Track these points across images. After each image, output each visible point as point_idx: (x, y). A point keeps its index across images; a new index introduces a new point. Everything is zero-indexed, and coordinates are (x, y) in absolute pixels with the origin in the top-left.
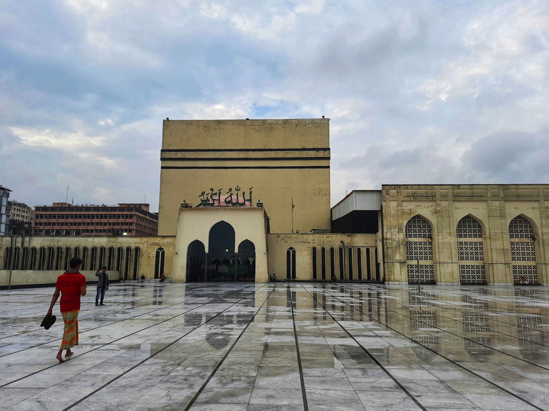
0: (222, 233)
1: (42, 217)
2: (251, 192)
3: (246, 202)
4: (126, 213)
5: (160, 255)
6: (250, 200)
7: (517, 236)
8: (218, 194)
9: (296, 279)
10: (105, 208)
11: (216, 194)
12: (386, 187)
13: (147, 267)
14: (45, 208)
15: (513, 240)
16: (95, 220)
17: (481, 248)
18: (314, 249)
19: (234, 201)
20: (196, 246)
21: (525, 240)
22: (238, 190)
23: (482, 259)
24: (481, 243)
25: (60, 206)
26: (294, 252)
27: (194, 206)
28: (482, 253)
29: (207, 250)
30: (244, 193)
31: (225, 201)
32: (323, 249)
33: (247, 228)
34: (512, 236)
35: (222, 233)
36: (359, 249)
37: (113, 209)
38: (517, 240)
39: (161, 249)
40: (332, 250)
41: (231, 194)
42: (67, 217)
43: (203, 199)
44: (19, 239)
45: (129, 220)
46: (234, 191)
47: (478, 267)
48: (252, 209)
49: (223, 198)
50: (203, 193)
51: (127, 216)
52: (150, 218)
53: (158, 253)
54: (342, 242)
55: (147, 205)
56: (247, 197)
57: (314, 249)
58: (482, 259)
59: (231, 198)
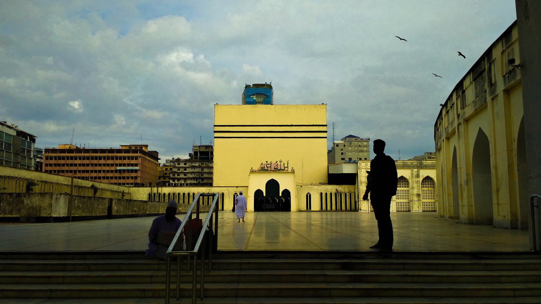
0: (272, 185)
1: (51, 159)
4: (131, 155)
6: (287, 167)
7: (426, 187)
10: (111, 151)
12: (360, 161)
14: (54, 151)
15: (424, 189)
16: (102, 162)
17: (408, 193)
18: (321, 194)
20: (258, 193)
21: (430, 189)
23: (408, 199)
24: (408, 191)
25: (67, 147)
26: (310, 195)
28: (408, 196)
29: (265, 195)
32: (326, 194)
33: (285, 183)
34: (424, 187)
35: (272, 185)
36: (346, 194)
37: (119, 151)
38: (426, 189)
40: (331, 194)
42: (76, 159)
44: (156, 189)
45: (133, 162)
46: (279, 163)
47: (406, 203)
48: (288, 172)
49: (273, 167)
50: (262, 164)
55: (146, 146)
56: (286, 166)
57: (321, 194)
58: (408, 199)
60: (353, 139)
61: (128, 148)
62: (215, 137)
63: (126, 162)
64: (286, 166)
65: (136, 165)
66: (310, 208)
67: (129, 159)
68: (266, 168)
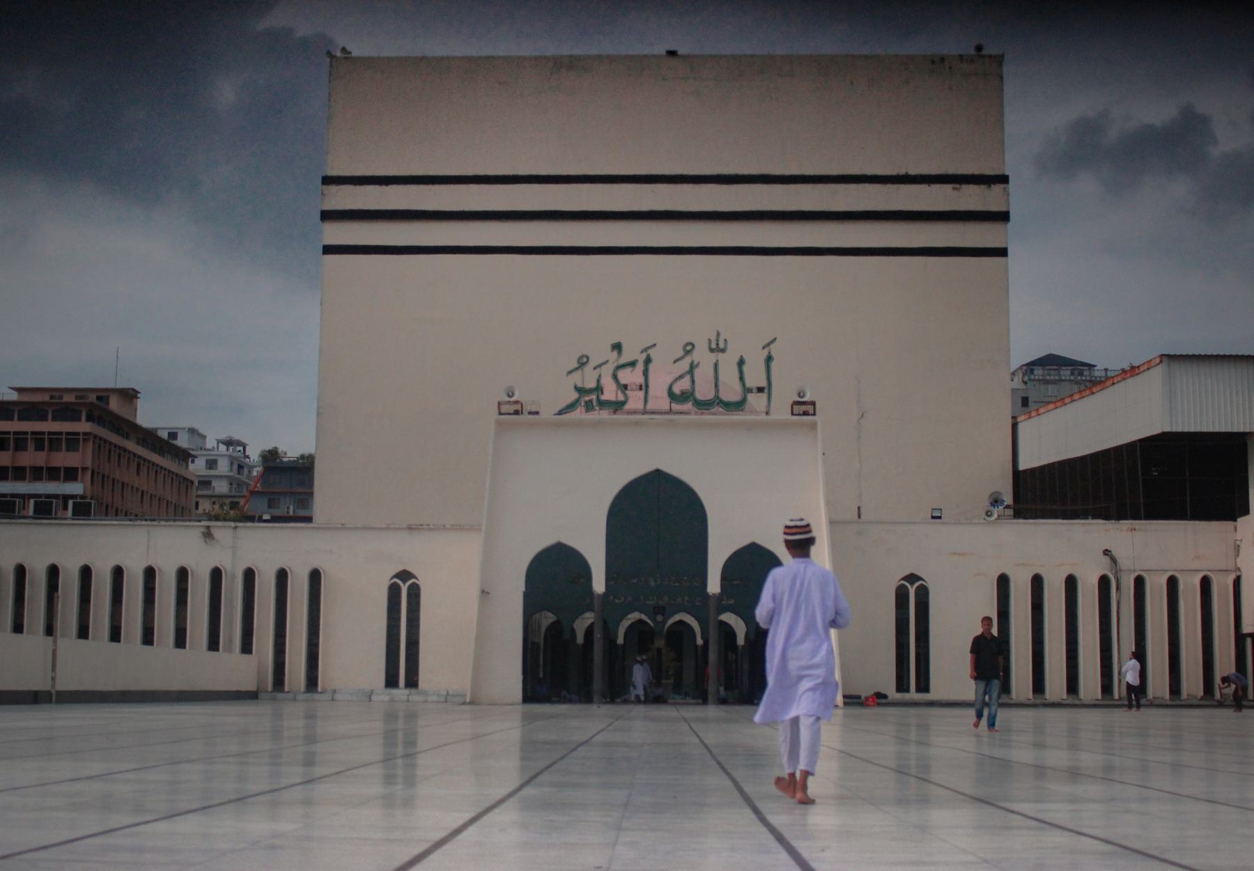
0: (657, 514)
2: (769, 359)
3: (750, 397)
5: (404, 600)
8: (640, 367)
9: (933, 695)
11: (633, 364)
13: (354, 648)
19: (704, 391)
22: (717, 349)
26: (923, 594)
27: (547, 413)
30: (741, 363)
31: (672, 395)
35: (657, 514)
36: (1172, 583)
39: (404, 575)
41: (692, 367)
43: (579, 385)
45: (63, 459)
46: (703, 357)
50: (582, 362)
51: (52, 442)
52: (141, 451)
53: (394, 592)
54: (1106, 552)
55: (130, 395)
59: (693, 382)
60: (1066, 373)
61: (46, 398)
62: (329, 250)
63: (30, 457)
64: (755, 377)
65: (71, 474)
66: (923, 686)
67: (39, 447)
68: (610, 393)
